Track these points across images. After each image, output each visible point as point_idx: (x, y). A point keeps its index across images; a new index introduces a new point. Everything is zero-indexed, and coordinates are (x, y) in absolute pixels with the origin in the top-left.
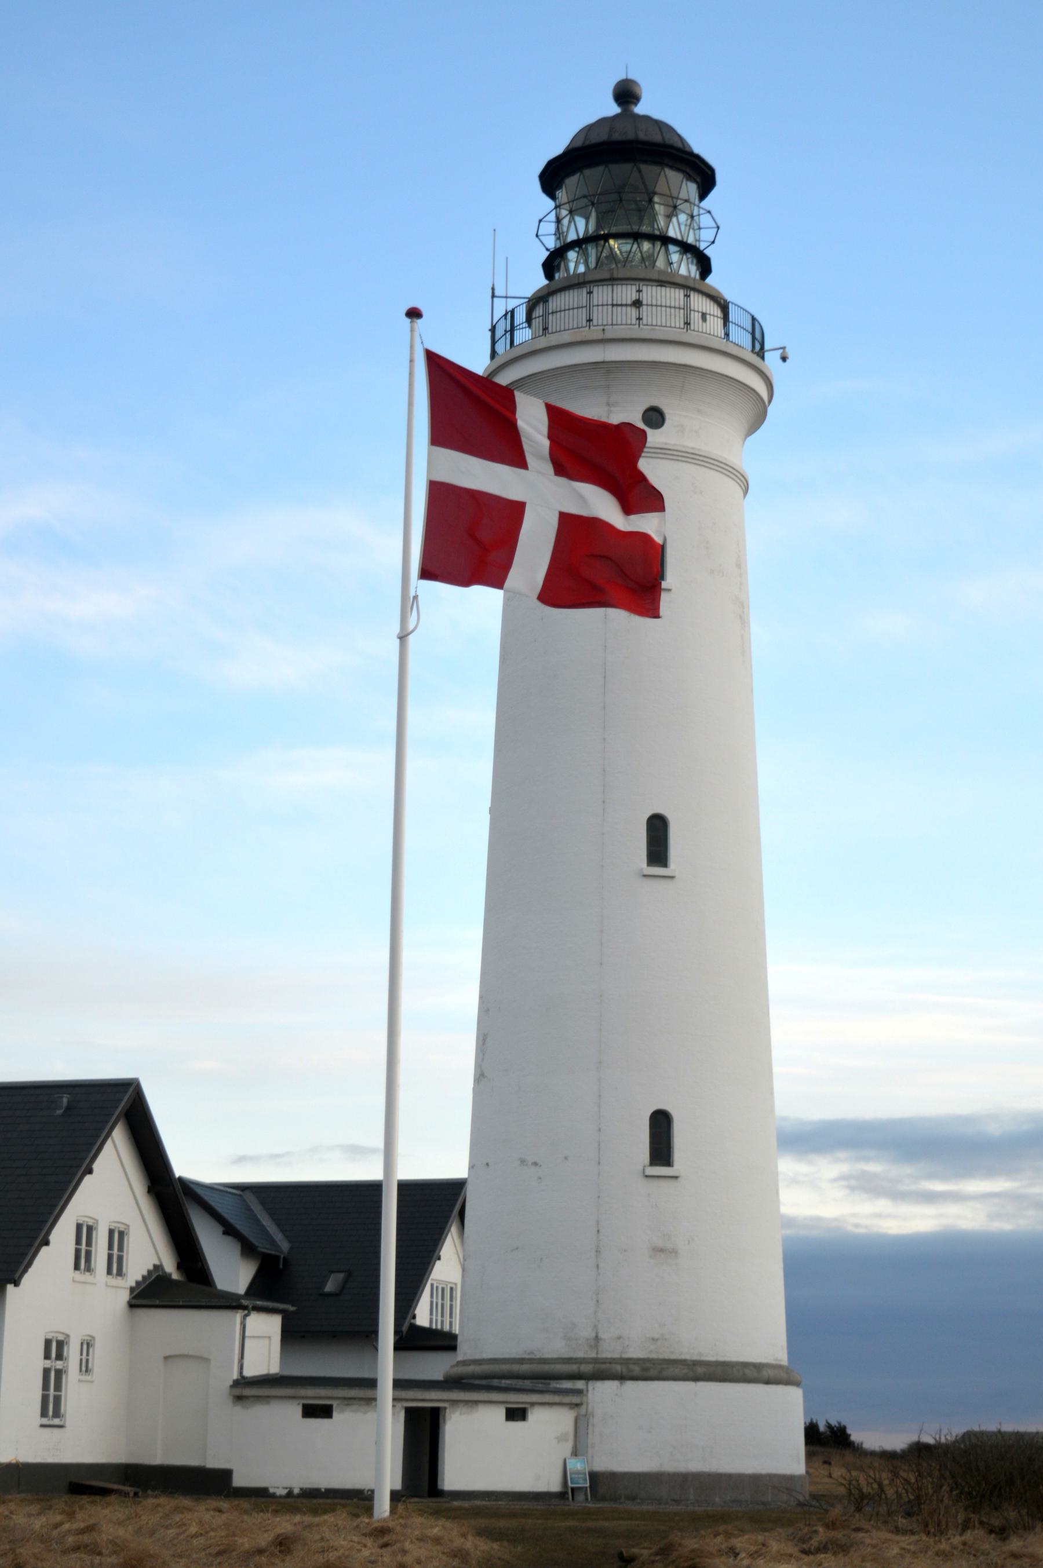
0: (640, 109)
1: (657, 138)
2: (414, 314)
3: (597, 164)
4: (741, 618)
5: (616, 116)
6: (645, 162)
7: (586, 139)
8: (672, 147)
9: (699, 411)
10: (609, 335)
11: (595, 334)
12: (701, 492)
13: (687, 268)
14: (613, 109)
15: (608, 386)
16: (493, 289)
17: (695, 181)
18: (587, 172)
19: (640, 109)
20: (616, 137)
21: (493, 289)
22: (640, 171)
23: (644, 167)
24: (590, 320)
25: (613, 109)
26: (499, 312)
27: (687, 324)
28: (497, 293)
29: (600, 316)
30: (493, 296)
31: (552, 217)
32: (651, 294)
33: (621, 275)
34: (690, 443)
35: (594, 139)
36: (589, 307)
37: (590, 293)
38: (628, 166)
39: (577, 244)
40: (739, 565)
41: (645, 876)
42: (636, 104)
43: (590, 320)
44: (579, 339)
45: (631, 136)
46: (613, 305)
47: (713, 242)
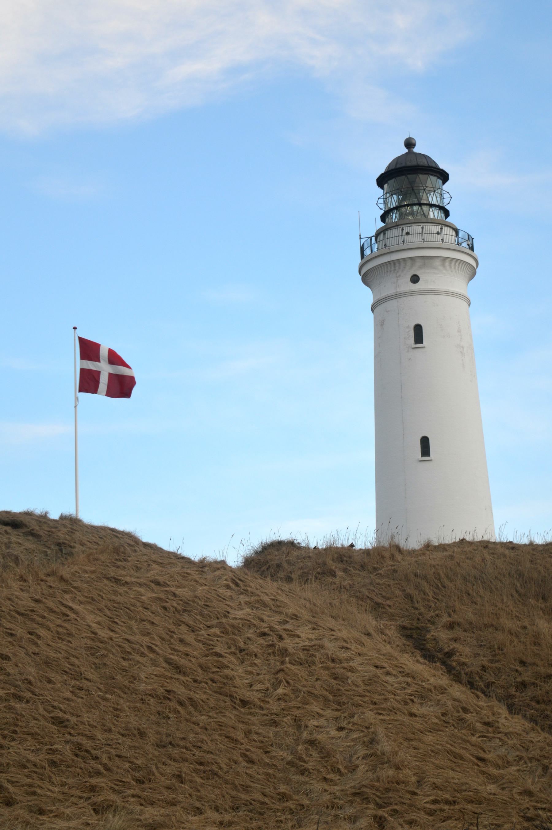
0: (416, 150)
1: (414, 163)
2: (75, 328)
3: (392, 178)
4: (461, 352)
5: (406, 153)
6: (410, 174)
7: (388, 168)
8: (419, 166)
9: (434, 273)
10: (391, 250)
11: (386, 250)
12: (437, 305)
13: (434, 214)
14: (406, 151)
15: (395, 270)
16: (360, 235)
17: (435, 176)
18: (389, 182)
19: (416, 150)
20: (398, 166)
21: (360, 235)
22: (408, 178)
23: (409, 176)
24: (385, 245)
25: (406, 151)
26: (362, 244)
27: (423, 239)
28: (362, 237)
29: (388, 242)
30: (360, 238)
31: (381, 201)
32: (407, 229)
33: (399, 224)
34: (431, 287)
35: (391, 169)
36: (385, 239)
37: (384, 234)
38: (404, 177)
39: (396, 208)
40: (459, 331)
41: (420, 461)
42: (414, 148)
43: (385, 245)
44: (381, 253)
45: (404, 165)
46: (398, 236)
47: (451, 198)
